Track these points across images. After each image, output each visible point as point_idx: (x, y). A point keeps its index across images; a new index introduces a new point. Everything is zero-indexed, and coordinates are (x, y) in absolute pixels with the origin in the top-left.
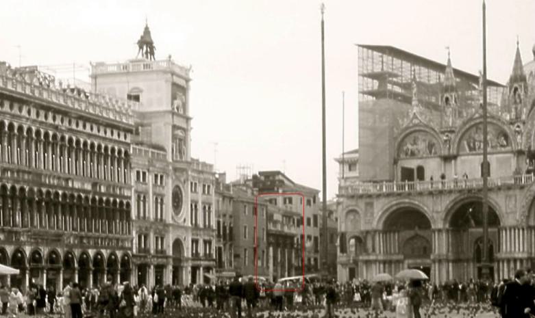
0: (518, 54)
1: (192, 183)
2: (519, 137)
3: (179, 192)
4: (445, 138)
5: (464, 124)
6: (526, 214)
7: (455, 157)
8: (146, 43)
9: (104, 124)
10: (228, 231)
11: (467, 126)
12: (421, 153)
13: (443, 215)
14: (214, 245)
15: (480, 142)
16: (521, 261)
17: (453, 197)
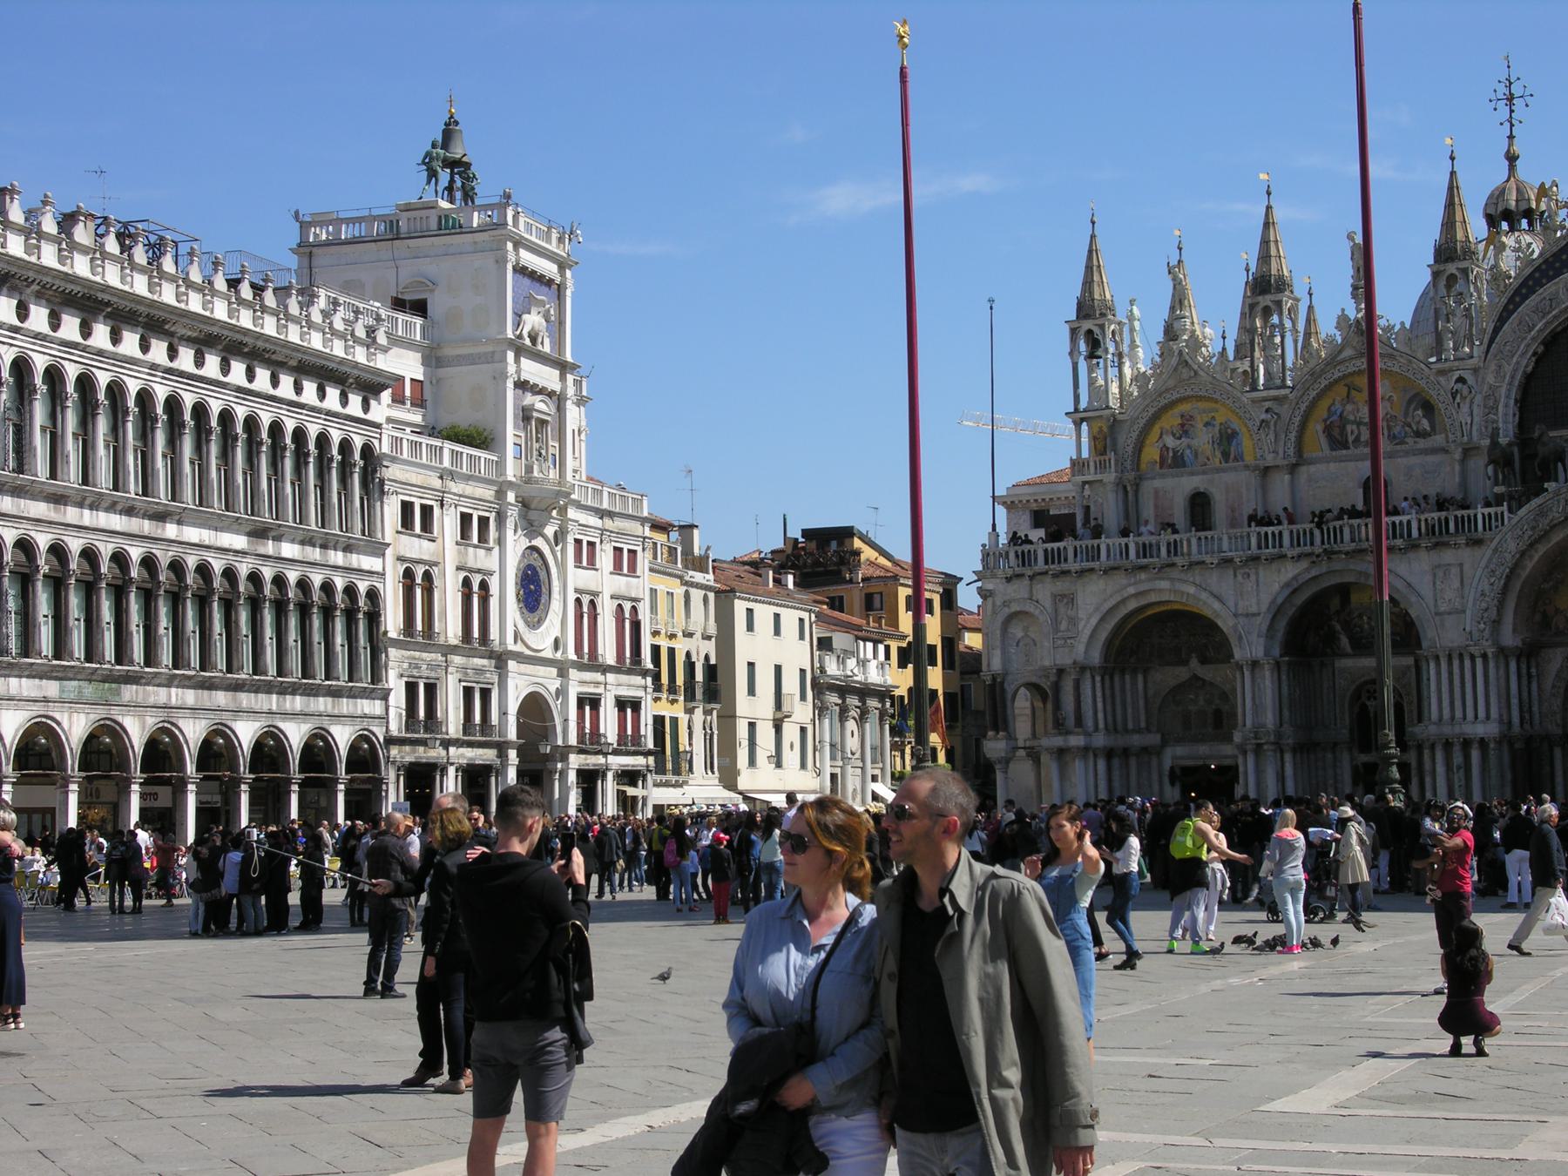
0: (1452, 189)
1: (578, 542)
2: (1465, 408)
3: (538, 564)
4: (1264, 416)
5: (1314, 375)
6: (1493, 613)
7: (1293, 469)
8: (448, 165)
9: (293, 363)
10: (699, 677)
11: (1324, 383)
12: (1201, 459)
13: (1262, 623)
14: (648, 711)
15: (1359, 424)
16: (1483, 743)
17: (1289, 571)
